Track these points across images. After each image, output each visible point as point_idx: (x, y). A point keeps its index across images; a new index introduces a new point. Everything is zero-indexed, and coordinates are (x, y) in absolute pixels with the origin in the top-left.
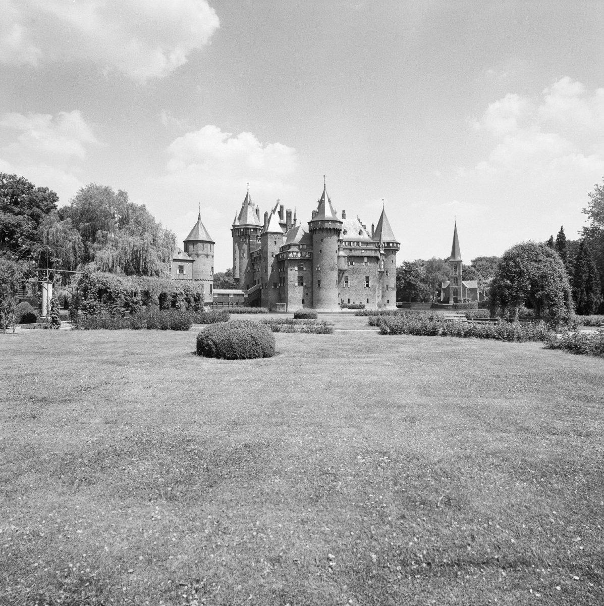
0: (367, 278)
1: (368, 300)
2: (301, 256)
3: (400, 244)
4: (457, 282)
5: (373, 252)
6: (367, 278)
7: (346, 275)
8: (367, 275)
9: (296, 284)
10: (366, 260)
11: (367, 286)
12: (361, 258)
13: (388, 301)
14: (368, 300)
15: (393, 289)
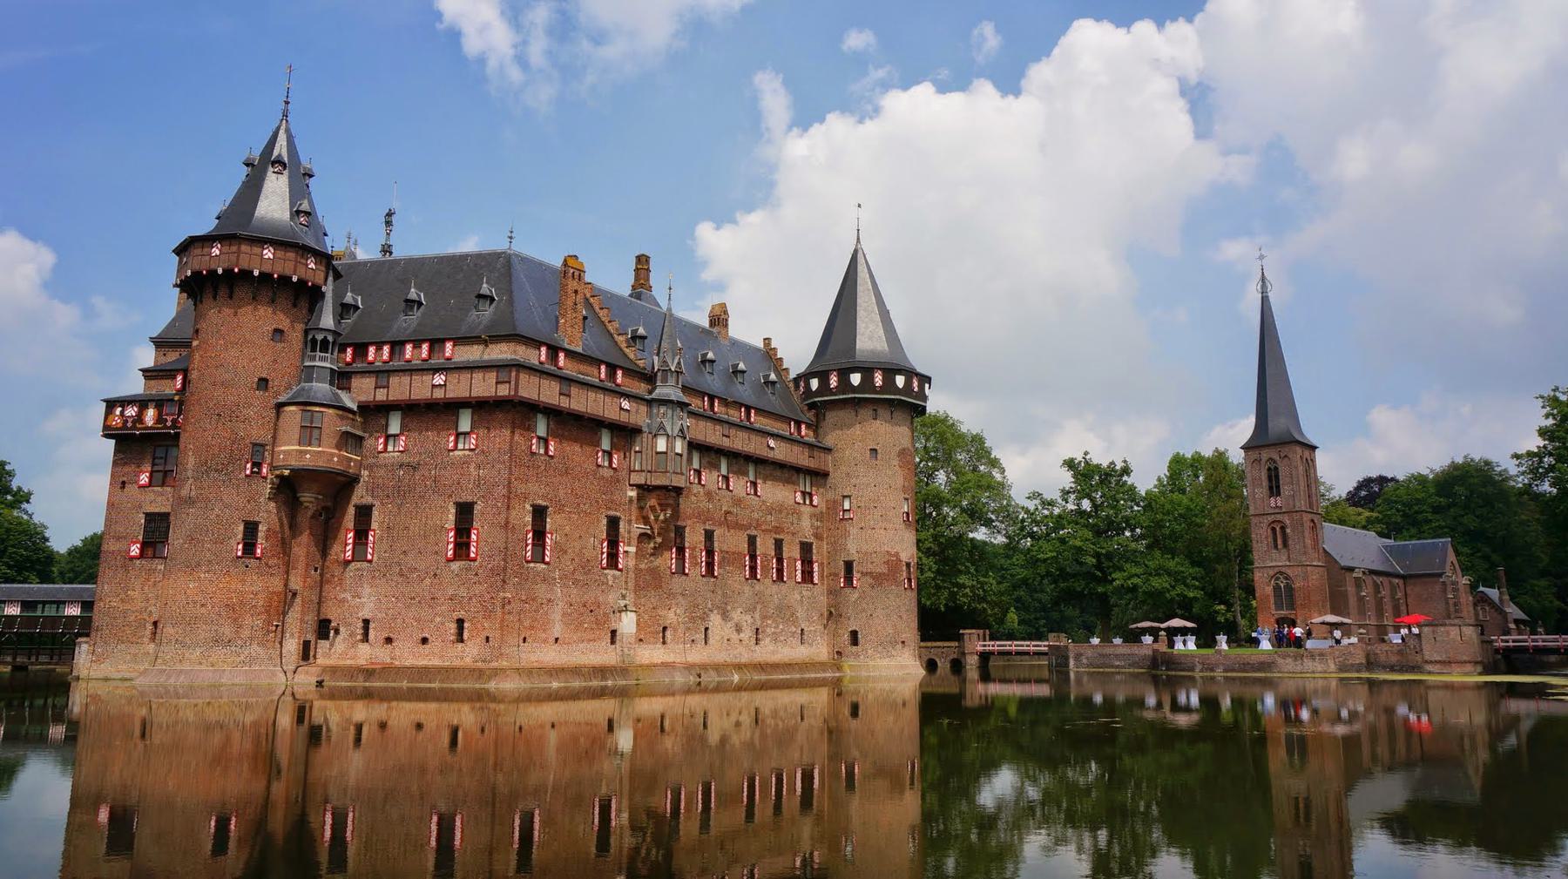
0: (465, 512)
1: (460, 622)
2: (160, 419)
3: (925, 379)
4: (1285, 545)
5: (492, 377)
6: (465, 512)
7: (360, 496)
8: (466, 497)
9: (135, 550)
10: (465, 424)
11: (462, 548)
12: (440, 412)
13: (854, 634)
14: (460, 622)
15: (878, 579)
